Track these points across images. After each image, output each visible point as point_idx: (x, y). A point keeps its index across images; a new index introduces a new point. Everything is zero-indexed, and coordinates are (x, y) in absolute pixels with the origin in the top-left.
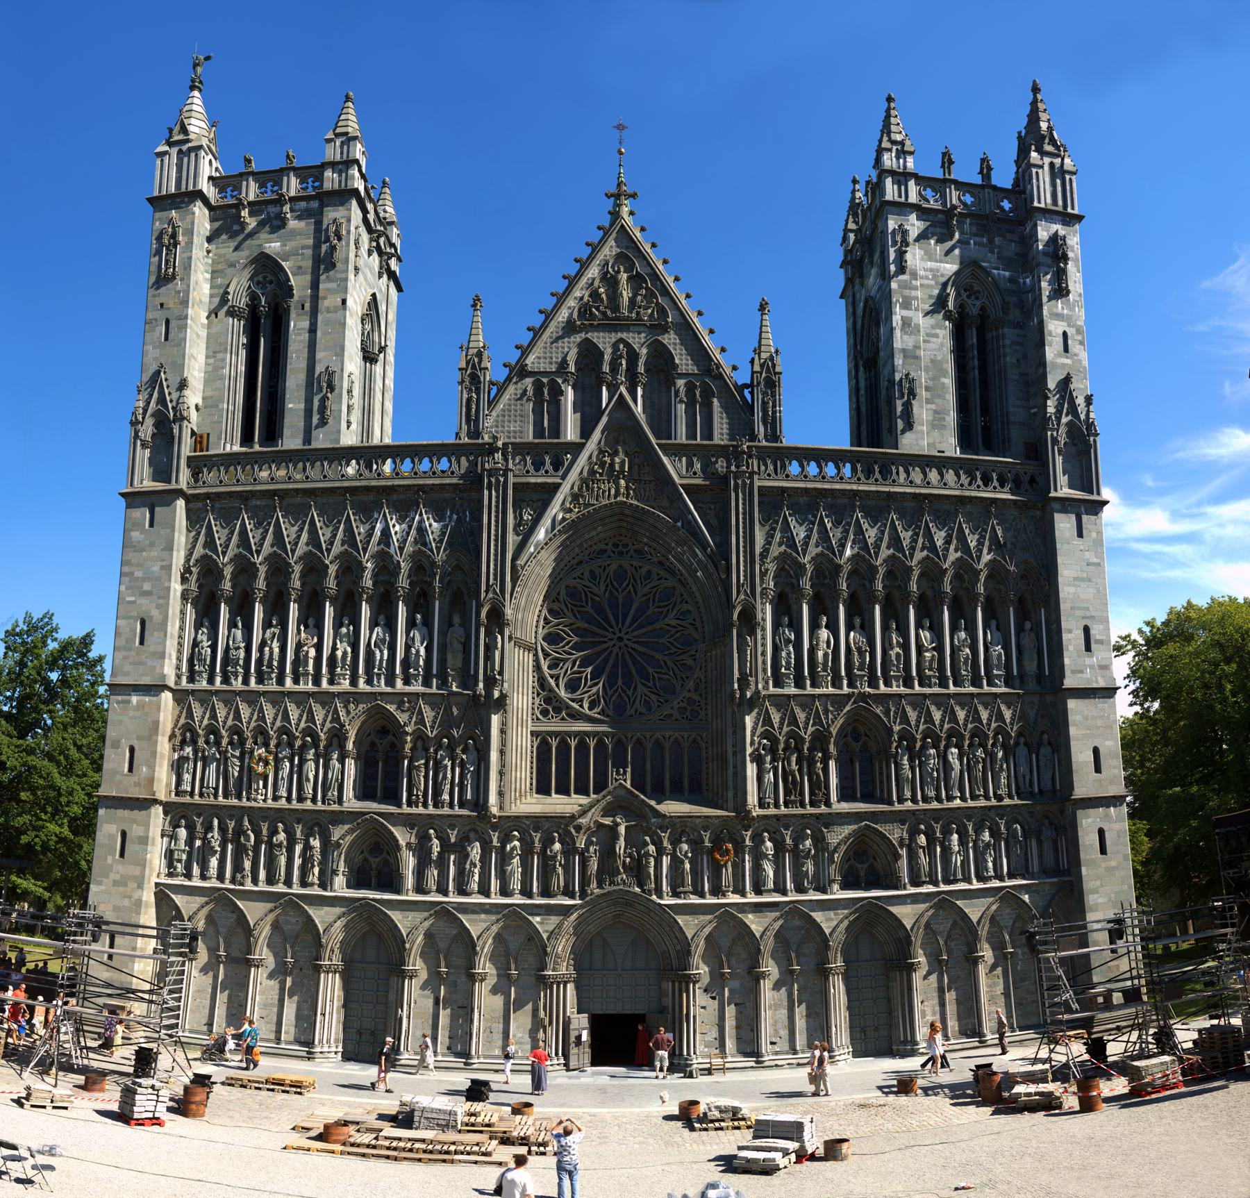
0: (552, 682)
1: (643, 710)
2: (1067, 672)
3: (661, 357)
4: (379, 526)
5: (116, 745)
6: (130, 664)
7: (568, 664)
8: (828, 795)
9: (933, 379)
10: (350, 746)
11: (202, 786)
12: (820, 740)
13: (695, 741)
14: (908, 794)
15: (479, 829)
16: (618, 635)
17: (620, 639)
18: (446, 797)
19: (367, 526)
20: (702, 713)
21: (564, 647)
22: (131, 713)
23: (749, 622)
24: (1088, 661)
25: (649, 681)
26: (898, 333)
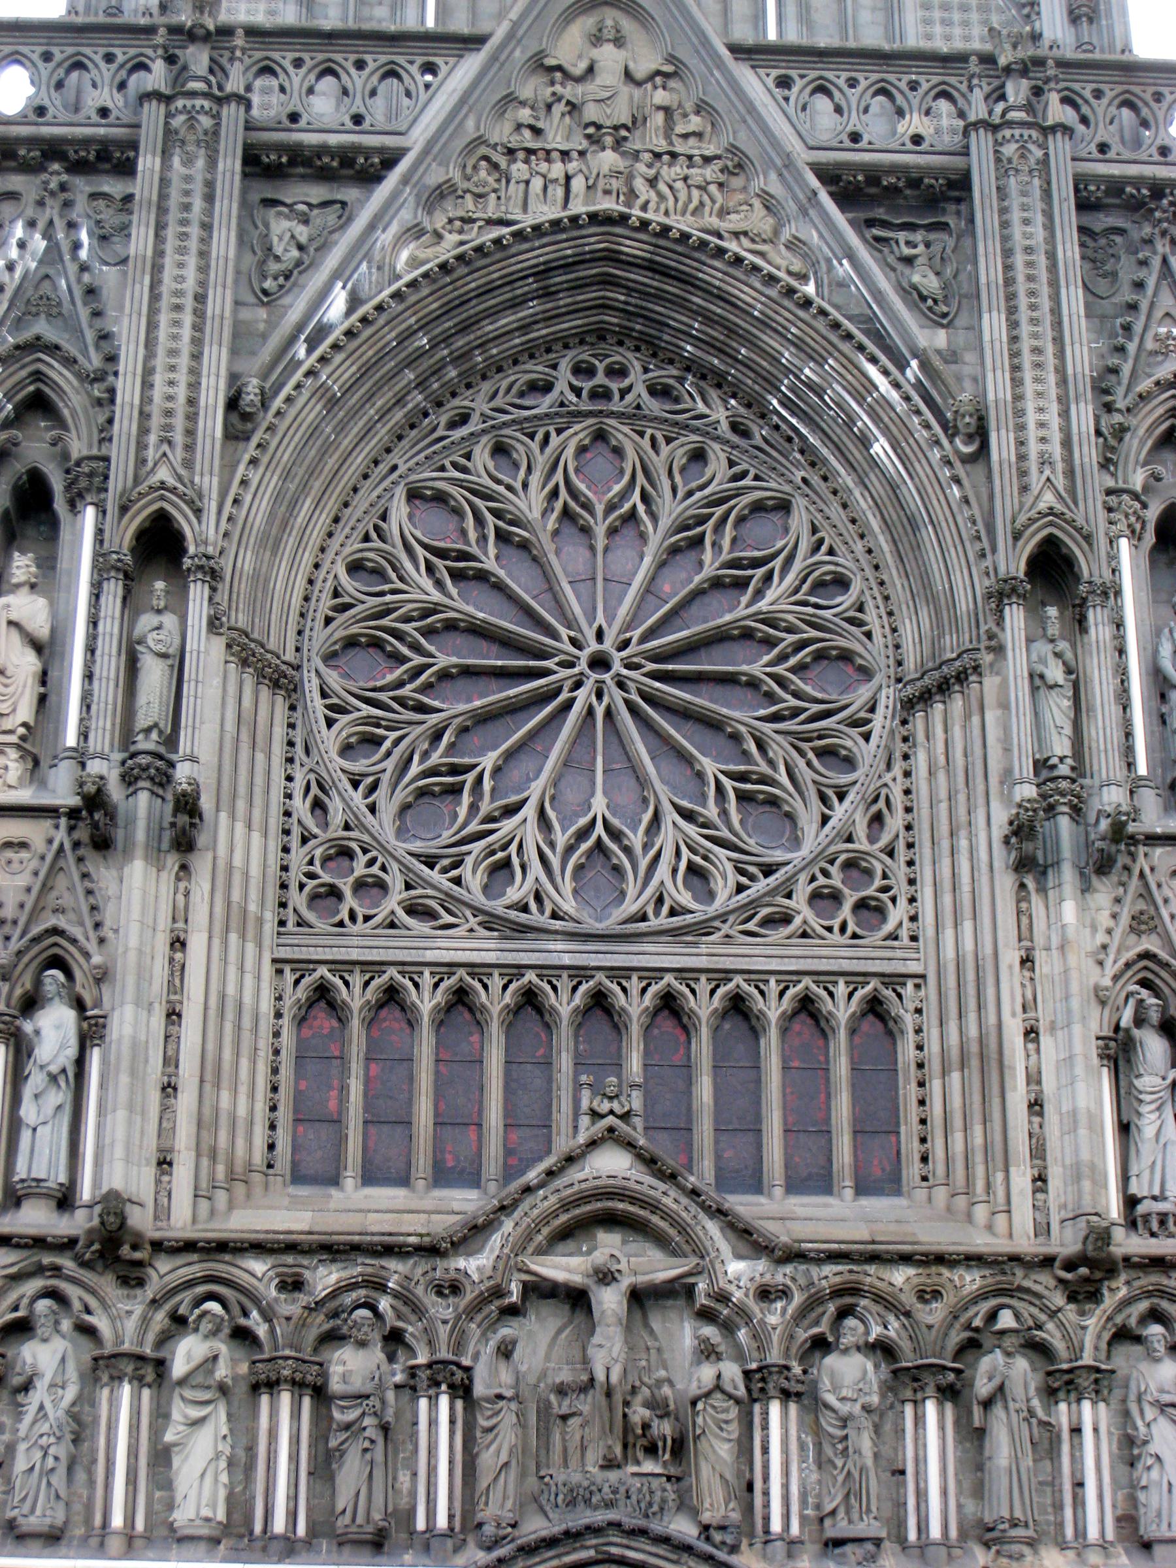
1: (685, 898)
13: (874, 1007)
15: (72, 1291)
16: (593, 646)
17: (600, 662)
20: (897, 914)
21: (400, 684)
25: (703, 798)
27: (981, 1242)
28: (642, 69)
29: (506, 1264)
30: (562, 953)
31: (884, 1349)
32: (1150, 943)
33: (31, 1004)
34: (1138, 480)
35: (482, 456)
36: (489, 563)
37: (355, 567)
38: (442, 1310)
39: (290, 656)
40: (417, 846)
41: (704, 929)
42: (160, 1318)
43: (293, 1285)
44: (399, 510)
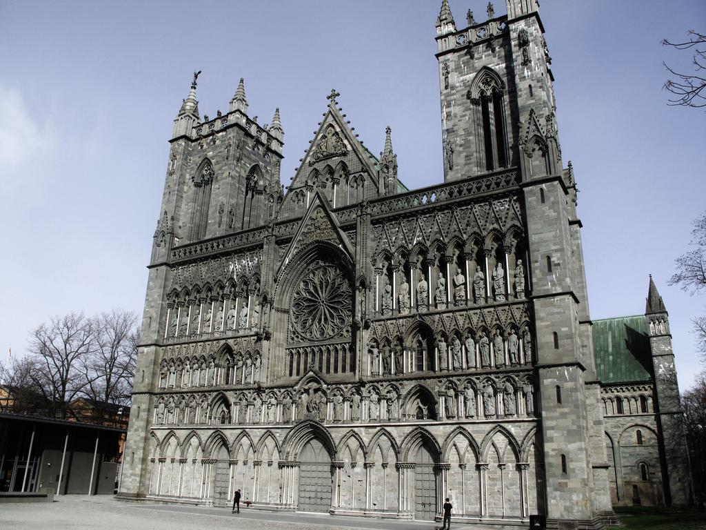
3: (344, 166)
17: (323, 302)
18: (248, 380)
22: (144, 357)
27: (353, 380)
28: (322, 216)
29: (300, 387)
30: (316, 343)
32: (375, 336)
33: (256, 359)
34: (381, 265)
35: (311, 275)
38: (294, 393)
39: (287, 308)
40: (303, 331)
41: (332, 338)
42: (268, 397)
43: (280, 392)
44: (302, 284)
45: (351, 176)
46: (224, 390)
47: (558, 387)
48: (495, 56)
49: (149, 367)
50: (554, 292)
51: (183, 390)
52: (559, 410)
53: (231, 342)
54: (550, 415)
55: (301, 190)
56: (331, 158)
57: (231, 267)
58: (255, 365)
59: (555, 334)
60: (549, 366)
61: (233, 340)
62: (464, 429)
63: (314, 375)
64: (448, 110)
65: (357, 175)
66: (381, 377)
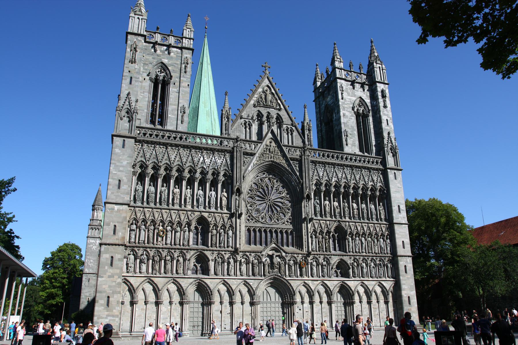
0: (250, 211)
1: (276, 221)
2: (394, 218)
3: (279, 118)
4: (202, 159)
5: (108, 224)
6: (114, 195)
7: (255, 206)
8: (330, 249)
9: (352, 131)
10: (192, 227)
11: (139, 240)
12: (329, 232)
14: (351, 250)
17: (270, 200)
19: (197, 159)
23: (309, 197)
24: (400, 215)
26: (342, 118)
30: (267, 226)
31: (294, 261)
36: (261, 190)
37: (249, 190)
41: (278, 224)
45: (285, 126)
46: (204, 250)
47: (405, 266)
48: (364, 94)
49: (122, 222)
50: (402, 223)
51: (157, 246)
52: (406, 276)
53: (206, 215)
54: (403, 278)
55: (249, 121)
56: (270, 108)
57: (202, 159)
58: (228, 234)
59: (403, 242)
60: (402, 256)
61: (207, 214)
62: (363, 283)
63: (276, 247)
64: (344, 112)
65: (289, 126)
66: (318, 253)
